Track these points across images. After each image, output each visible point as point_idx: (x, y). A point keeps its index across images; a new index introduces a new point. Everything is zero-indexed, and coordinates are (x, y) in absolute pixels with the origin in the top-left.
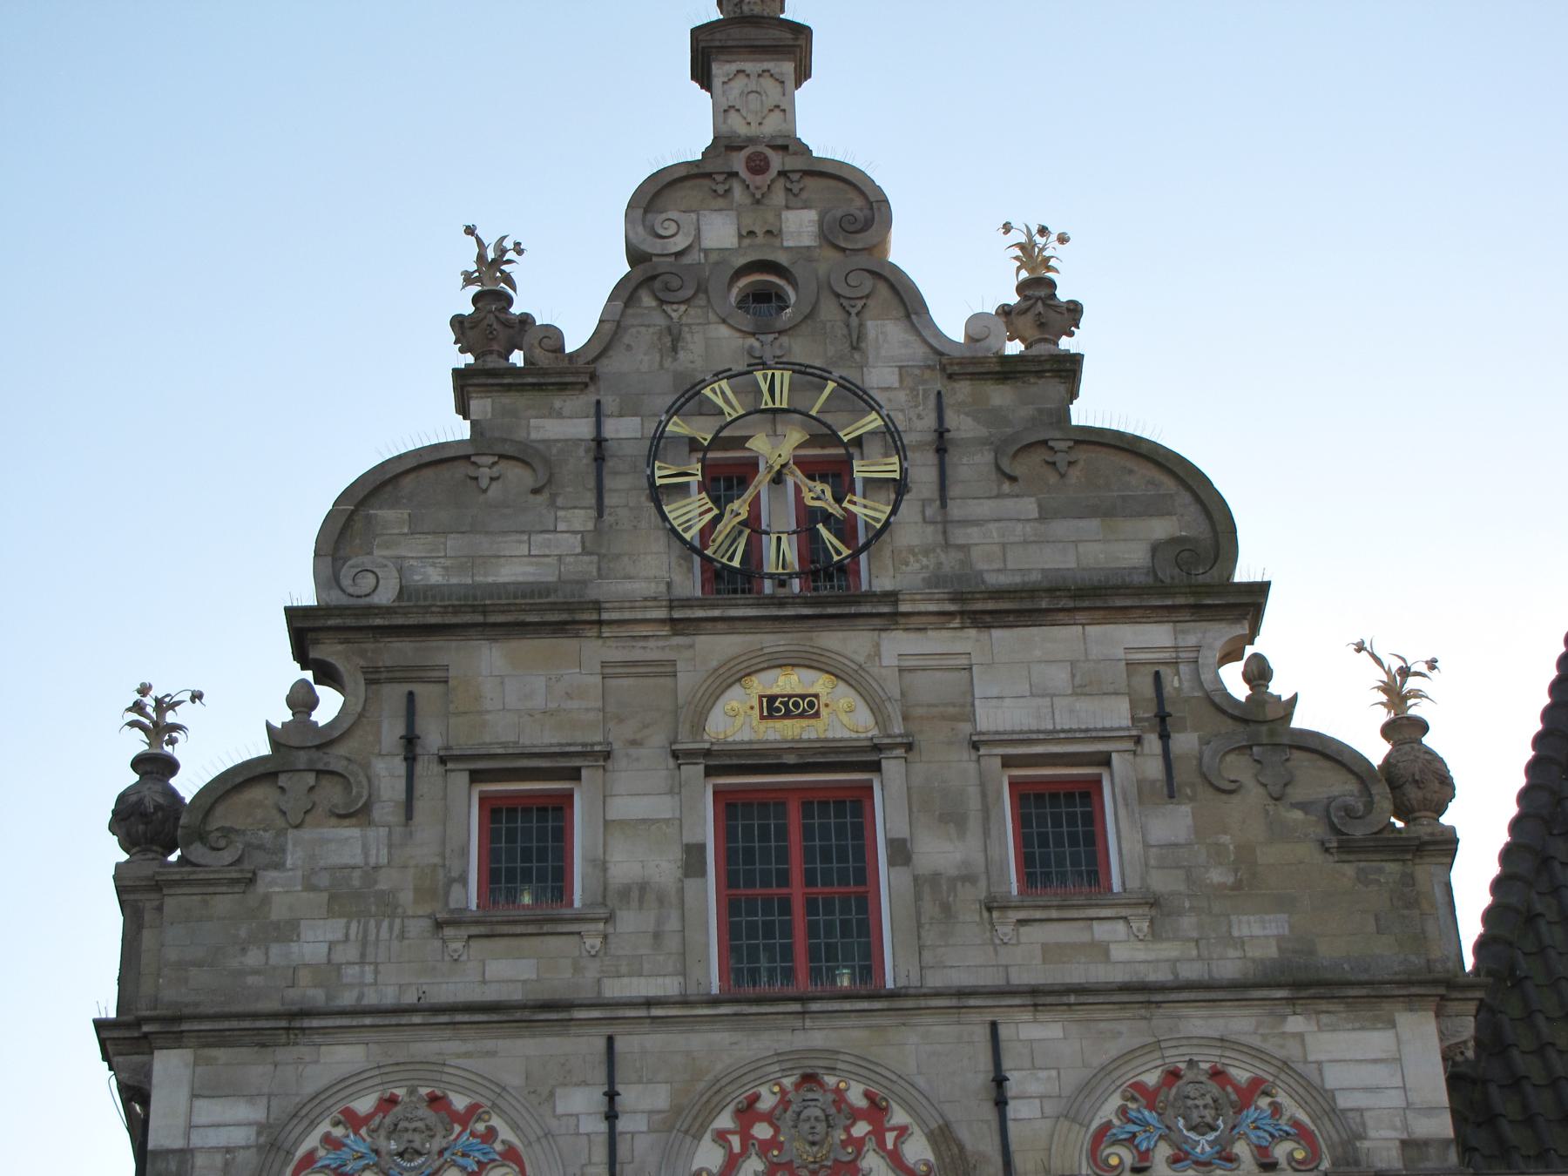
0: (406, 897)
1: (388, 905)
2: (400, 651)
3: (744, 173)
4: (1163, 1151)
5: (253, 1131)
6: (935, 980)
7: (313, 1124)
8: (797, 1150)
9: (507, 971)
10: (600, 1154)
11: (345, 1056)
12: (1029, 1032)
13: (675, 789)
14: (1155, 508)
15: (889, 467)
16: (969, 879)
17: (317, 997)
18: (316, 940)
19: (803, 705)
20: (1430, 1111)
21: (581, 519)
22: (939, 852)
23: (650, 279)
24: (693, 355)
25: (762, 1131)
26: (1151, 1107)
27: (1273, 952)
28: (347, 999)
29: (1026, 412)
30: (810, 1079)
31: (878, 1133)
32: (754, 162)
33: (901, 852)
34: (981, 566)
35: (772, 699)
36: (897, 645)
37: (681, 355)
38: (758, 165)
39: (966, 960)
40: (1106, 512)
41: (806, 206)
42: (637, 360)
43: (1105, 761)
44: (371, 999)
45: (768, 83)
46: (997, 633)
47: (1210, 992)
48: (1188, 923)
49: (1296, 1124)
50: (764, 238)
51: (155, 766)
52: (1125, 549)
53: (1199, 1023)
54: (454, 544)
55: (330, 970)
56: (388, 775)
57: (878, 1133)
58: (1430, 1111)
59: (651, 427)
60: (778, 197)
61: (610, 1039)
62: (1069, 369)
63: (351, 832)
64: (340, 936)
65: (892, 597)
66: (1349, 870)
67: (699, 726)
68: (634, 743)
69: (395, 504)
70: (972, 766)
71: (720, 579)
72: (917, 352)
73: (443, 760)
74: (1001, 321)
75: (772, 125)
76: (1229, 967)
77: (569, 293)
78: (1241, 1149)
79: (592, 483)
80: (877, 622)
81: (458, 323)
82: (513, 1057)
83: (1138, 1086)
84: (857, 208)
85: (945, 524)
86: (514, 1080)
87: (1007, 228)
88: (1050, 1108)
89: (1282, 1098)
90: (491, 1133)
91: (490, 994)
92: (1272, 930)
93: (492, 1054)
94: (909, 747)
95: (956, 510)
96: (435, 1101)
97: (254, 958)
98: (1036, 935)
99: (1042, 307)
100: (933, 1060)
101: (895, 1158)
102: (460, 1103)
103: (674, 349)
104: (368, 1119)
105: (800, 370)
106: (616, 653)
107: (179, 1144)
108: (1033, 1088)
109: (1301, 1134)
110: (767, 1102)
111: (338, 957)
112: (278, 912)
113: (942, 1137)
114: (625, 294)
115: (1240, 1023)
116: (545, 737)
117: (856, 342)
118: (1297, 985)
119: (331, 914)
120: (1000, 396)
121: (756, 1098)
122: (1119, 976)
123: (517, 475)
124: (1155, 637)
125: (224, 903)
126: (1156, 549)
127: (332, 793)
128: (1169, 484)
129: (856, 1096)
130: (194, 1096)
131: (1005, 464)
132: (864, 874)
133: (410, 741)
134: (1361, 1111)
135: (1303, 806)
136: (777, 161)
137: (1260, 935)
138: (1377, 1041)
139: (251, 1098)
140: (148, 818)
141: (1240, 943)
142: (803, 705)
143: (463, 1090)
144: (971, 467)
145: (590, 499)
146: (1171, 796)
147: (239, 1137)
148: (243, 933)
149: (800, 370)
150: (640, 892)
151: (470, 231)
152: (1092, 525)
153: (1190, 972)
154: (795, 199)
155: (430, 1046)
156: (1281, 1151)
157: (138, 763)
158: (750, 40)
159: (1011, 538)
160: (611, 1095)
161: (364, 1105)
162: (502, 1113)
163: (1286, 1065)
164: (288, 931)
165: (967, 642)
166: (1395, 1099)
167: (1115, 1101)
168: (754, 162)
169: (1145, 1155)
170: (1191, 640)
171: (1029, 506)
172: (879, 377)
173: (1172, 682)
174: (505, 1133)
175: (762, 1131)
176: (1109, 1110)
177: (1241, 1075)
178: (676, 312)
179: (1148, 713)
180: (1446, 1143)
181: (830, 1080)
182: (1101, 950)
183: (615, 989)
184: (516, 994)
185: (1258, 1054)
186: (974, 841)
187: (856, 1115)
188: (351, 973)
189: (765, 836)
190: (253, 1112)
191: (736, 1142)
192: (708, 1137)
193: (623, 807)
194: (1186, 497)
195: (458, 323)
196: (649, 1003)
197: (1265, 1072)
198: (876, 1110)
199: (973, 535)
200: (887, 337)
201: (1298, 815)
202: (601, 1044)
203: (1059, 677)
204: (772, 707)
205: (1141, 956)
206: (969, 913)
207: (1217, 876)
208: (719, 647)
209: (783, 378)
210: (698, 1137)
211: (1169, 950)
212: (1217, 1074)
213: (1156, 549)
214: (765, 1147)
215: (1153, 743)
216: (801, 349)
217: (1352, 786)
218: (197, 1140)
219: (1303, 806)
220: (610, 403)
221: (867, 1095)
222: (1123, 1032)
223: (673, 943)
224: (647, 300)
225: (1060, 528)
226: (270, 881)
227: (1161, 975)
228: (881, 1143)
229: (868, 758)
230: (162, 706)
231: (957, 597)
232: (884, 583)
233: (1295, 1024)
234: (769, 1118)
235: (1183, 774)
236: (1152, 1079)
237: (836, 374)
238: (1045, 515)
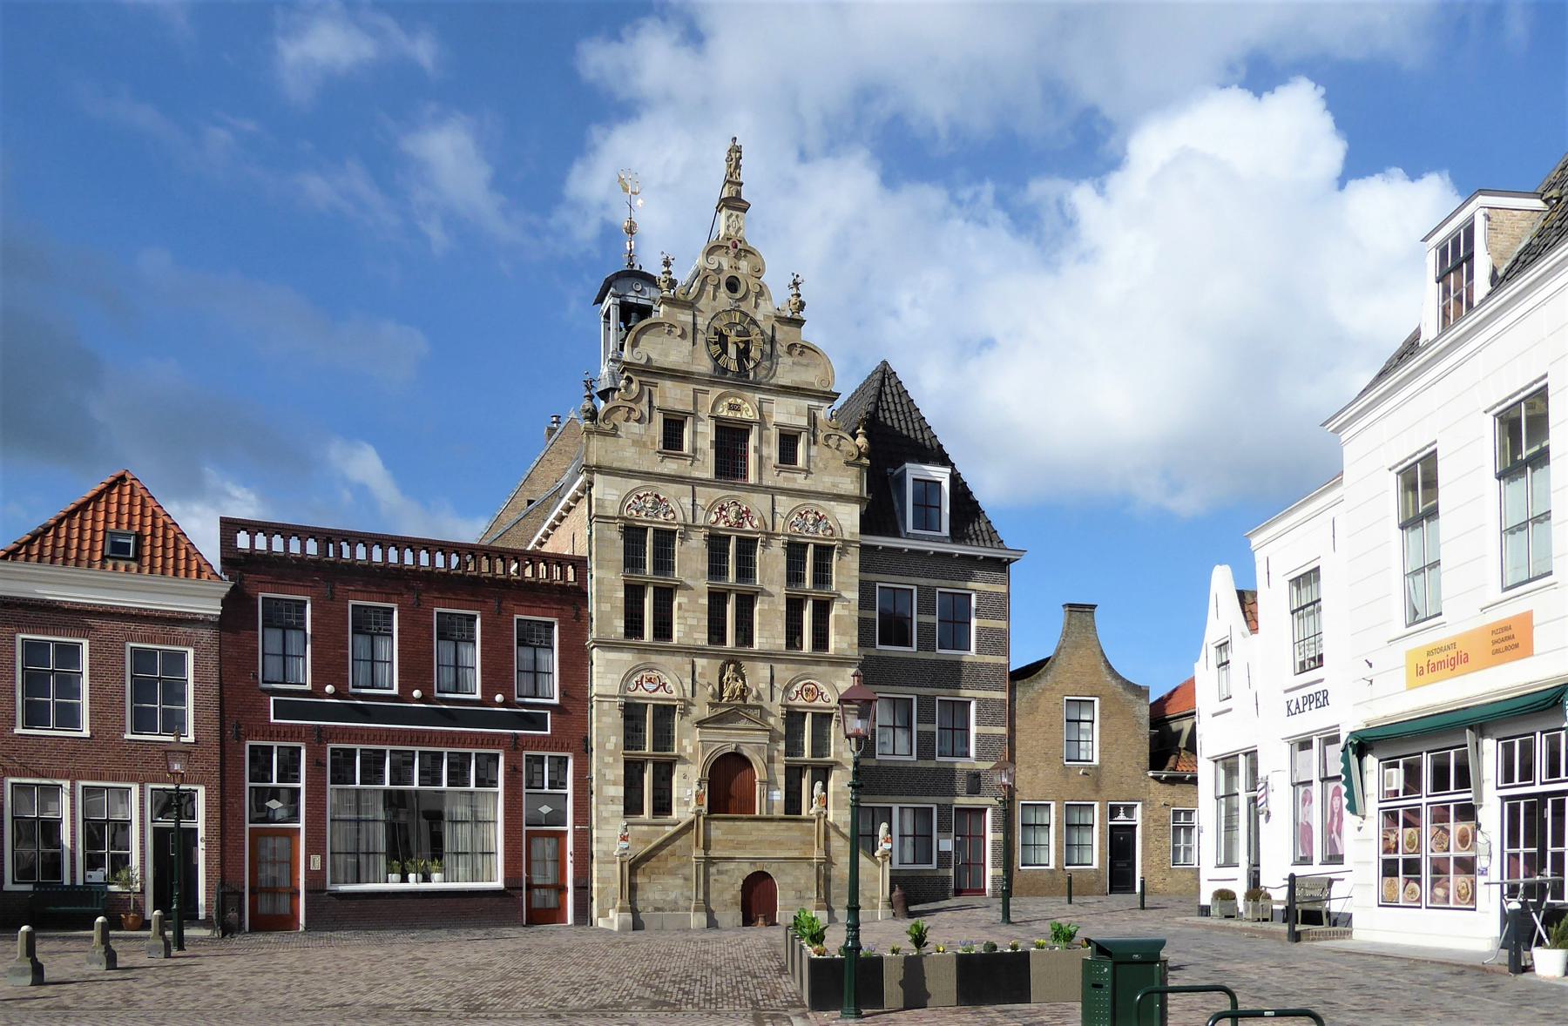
1: (645, 445)
9: (671, 467)
116: (679, 407)
183: (696, 474)
203: (793, 410)
204: (732, 407)
229: (750, 424)
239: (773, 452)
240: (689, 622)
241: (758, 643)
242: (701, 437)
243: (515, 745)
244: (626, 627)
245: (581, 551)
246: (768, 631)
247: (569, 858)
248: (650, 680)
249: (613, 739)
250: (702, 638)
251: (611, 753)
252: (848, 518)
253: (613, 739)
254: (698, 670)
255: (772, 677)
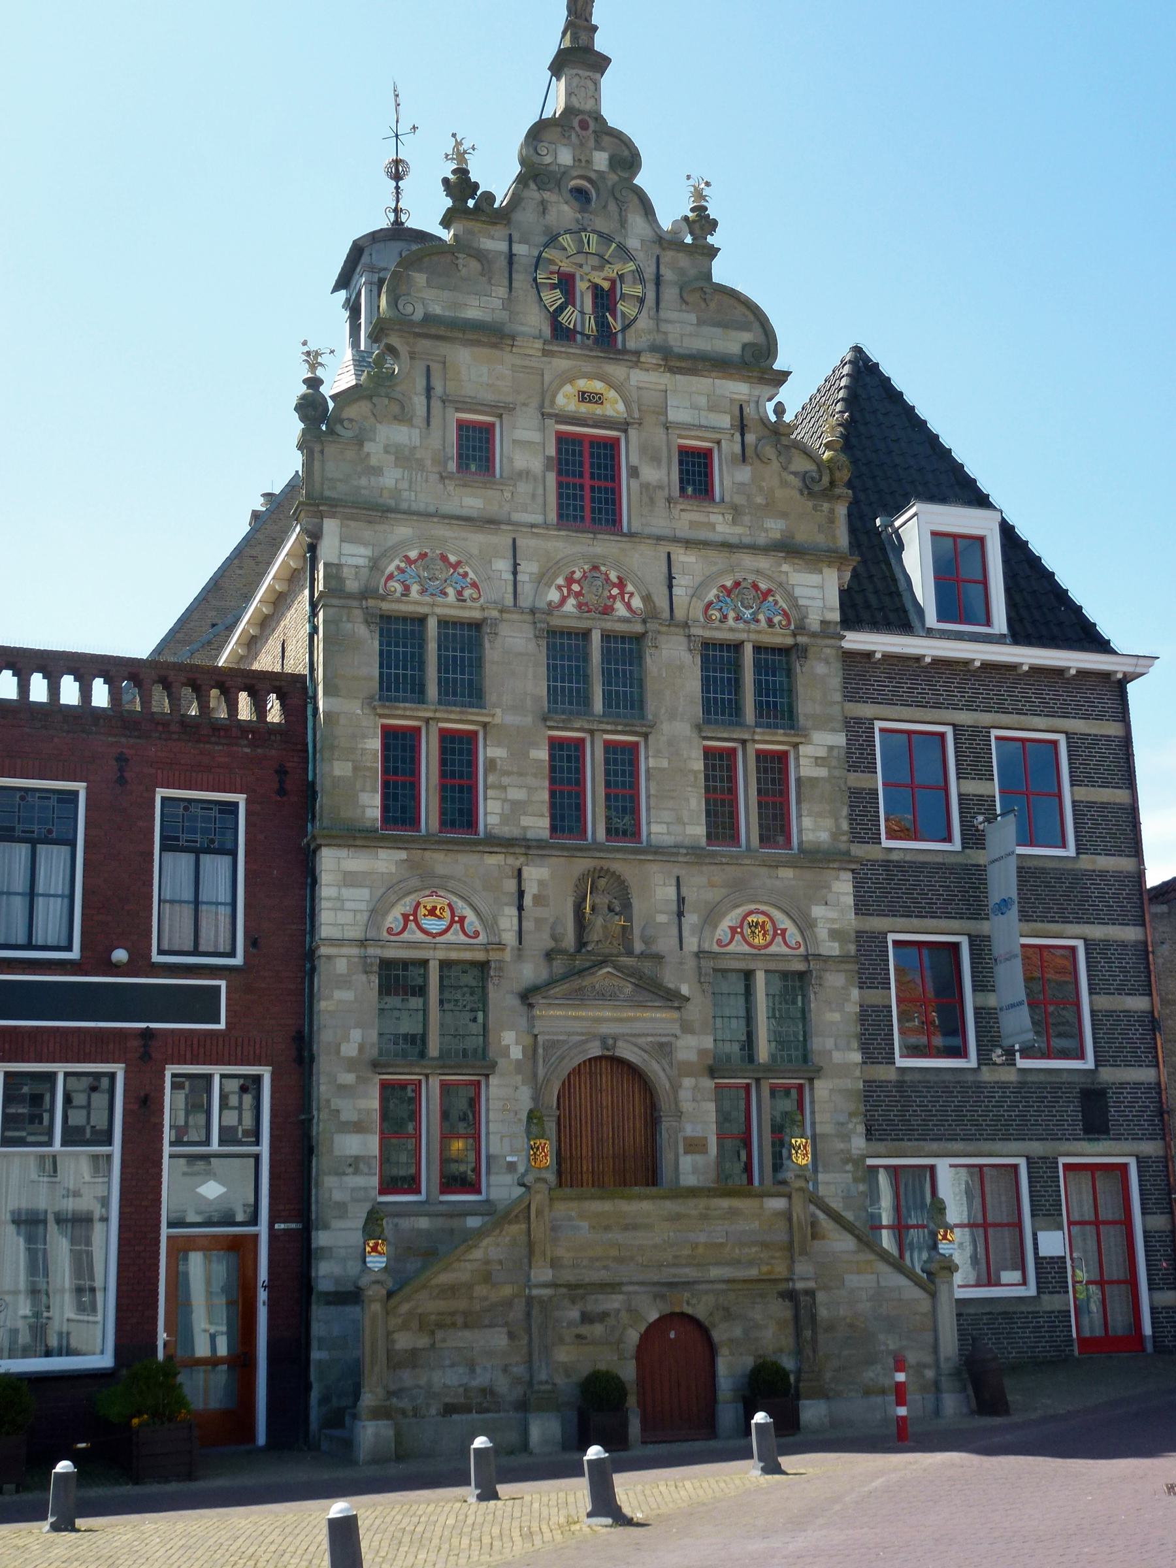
0: (428, 463)
2: (424, 344)
3: (577, 128)
4: (732, 615)
5: (367, 560)
6: (647, 530)
7: (392, 560)
8: (590, 598)
9: (472, 502)
10: (510, 589)
11: (402, 531)
12: (683, 558)
13: (543, 429)
14: (744, 327)
15: (638, 290)
16: (661, 487)
17: (392, 503)
18: (391, 477)
19: (597, 398)
20: (832, 609)
21: (502, 292)
22: (651, 474)
23: (533, 174)
24: (552, 218)
25: (576, 587)
26: (729, 596)
27: (778, 536)
28: (404, 506)
29: (693, 272)
30: (595, 568)
31: (622, 594)
32: (580, 123)
33: (634, 472)
34: (672, 343)
35: (584, 393)
36: (638, 377)
37: (547, 217)
38: (584, 126)
39: (659, 523)
40: (725, 325)
41: (603, 149)
42: (527, 216)
43: (719, 443)
44: (414, 507)
45: (590, 84)
46: (678, 377)
47: (753, 548)
48: (747, 519)
49: (783, 610)
50: (580, 159)
51: (314, 383)
52: (731, 343)
53: (749, 562)
54: (446, 294)
55: (396, 492)
56: (419, 402)
57: (622, 594)
58: (832, 609)
59: (536, 254)
60: (592, 143)
61: (514, 540)
62: (713, 252)
63: (404, 429)
64: (400, 476)
65: (638, 353)
66: (810, 504)
67: (553, 402)
68: (525, 405)
69: (420, 271)
70: (664, 437)
71: (561, 333)
72: (648, 233)
73: (444, 402)
74: (684, 225)
75: (589, 105)
76: (762, 540)
77: (497, 176)
78: (761, 617)
79: (507, 275)
80: (629, 364)
81: (446, 181)
82: (476, 541)
83: (723, 586)
84: (627, 159)
85: (658, 320)
86: (475, 552)
87: (689, 177)
88: (690, 592)
89: (778, 597)
90: (465, 575)
91: (465, 512)
92: (779, 527)
93: (465, 539)
94: (640, 424)
95: (663, 314)
96: (444, 558)
97: (363, 482)
98: (687, 516)
99: (701, 222)
100: (644, 562)
101: (628, 606)
102: (453, 559)
103: (544, 213)
104: (415, 561)
105: (600, 234)
106: (519, 362)
107: (336, 561)
108: (683, 583)
109: (786, 614)
110: (578, 575)
111: (400, 486)
112: (374, 461)
113: (647, 599)
114: (521, 180)
115: (763, 563)
116: (489, 397)
117: (623, 223)
118: (788, 552)
119: (396, 466)
120: (683, 261)
121: (574, 572)
122: (718, 538)
123: (474, 265)
124: (739, 389)
125: (350, 454)
126: (744, 346)
127: (395, 409)
128: (751, 317)
129: (613, 576)
130: (342, 541)
131: (685, 295)
132: (615, 477)
133: (429, 390)
134: (807, 607)
135: (795, 474)
136: (592, 124)
137: (774, 528)
138: (815, 579)
139: (365, 545)
140: (311, 407)
141: (766, 530)
142: (597, 398)
143: (454, 554)
144: (670, 294)
145: (506, 283)
146: (744, 460)
147: (361, 562)
148: (359, 469)
149: (600, 234)
150: (525, 474)
151: (454, 135)
152: (719, 331)
153: (747, 540)
154: (599, 147)
155: (441, 531)
156: (776, 619)
157: (306, 381)
158: (579, 57)
159: (684, 330)
160: (516, 565)
161: (413, 554)
162: (470, 566)
163: (781, 584)
164: (378, 471)
165: (664, 379)
166: (819, 603)
167: (714, 591)
168: (580, 123)
169: (725, 617)
170: (757, 393)
171: (693, 318)
172: (633, 243)
173: (747, 410)
174: (471, 575)
175: (576, 587)
176: (712, 594)
177: (763, 586)
178: (547, 195)
179: (737, 423)
180: (836, 623)
181: (603, 569)
182: (712, 526)
183: (517, 517)
184: (475, 514)
185: (770, 578)
186: (664, 471)
187: (614, 585)
188: (405, 494)
189: (574, 454)
190: (367, 552)
191: (565, 590)
192: (553, 588)
193: (522, 434)
194: (757, 325)
195: (446, 181)
196: (532, 526)
197: (773, 586)
198: (621, 585)
199: (668, 328)
200: (636, 222)
201: (792, 477)
202: (511, 542)
203: (703, 401)
204: (584, 397)
205: (728, 531)
206: (661, 503)
207: (759, 500)
208: (561, 364)
209: (594, 238)
210: (550, 587)
211: (738, 530)
212: (755, 586)
213: (744, 346)
214: (578, 595)
215: (738, 437)
216: (600, 224)
217: (814, 467)
218: (343, 561)
219: (795, 474)
220: (515, 237)
221: (619, 578)
222: (719, 560)
223: (540, 500)
224: (533, 186)
225: (706, 330)
226: (369, 447)
227: (734, 540)
228: (623, 599)
229: (624, 427)
230: (317, 354)
231: (665, 359)
232: (631, 345)
233: (785, 567)
234: (578, 582)
235: (749, 452)
236: (729, 584)
237: (617, 240)
238: (700, 322)
239: (662, 474)
240: (512, 797)
241: (657, 828)
242: (525, 448)
243: (146, 1055)
244: (385, 809)
245: (297, 663)
246: (674, 813)
247: (263, 1295)
248: (432, 912)
249: (356, 1035)
250: (538, 824)
251: (351, 1065)
252: (819, 592)
253: (356, 1035)
254: (531, 889)
255: (681, 900)
